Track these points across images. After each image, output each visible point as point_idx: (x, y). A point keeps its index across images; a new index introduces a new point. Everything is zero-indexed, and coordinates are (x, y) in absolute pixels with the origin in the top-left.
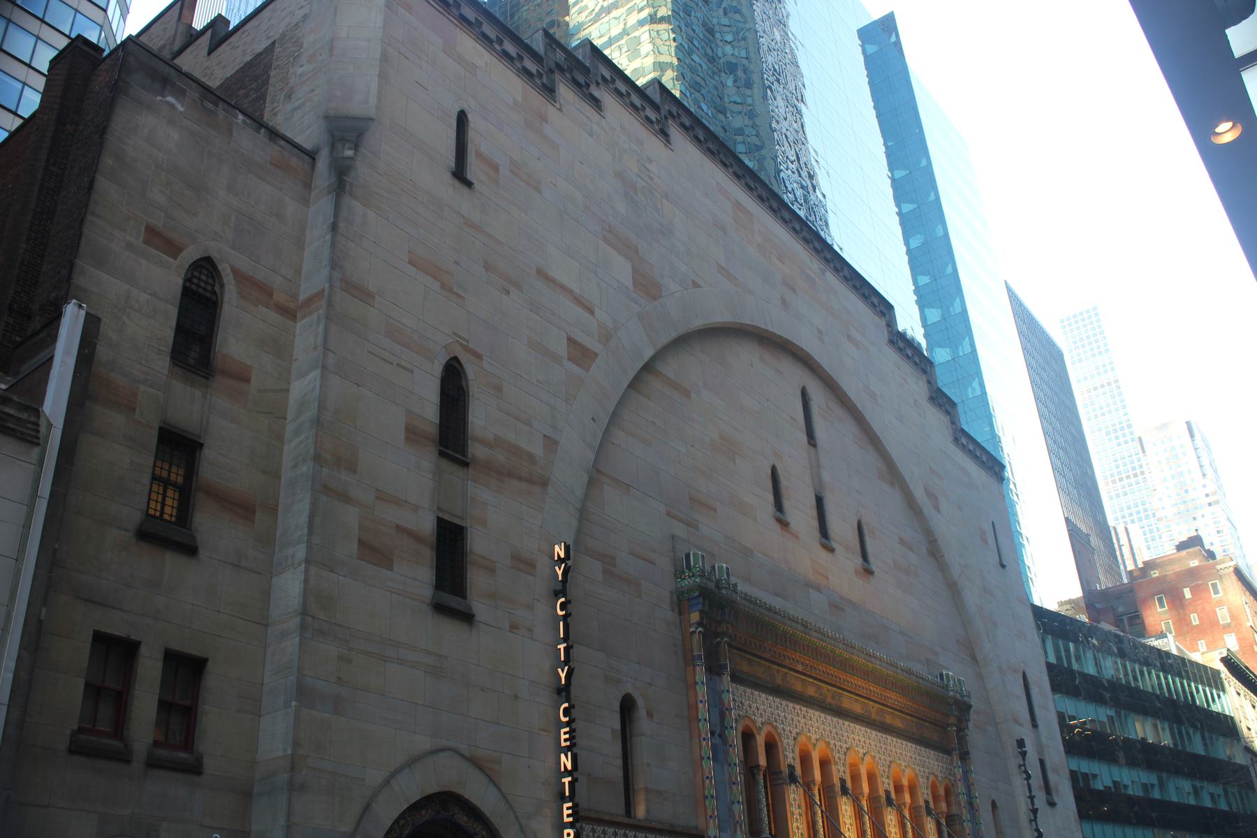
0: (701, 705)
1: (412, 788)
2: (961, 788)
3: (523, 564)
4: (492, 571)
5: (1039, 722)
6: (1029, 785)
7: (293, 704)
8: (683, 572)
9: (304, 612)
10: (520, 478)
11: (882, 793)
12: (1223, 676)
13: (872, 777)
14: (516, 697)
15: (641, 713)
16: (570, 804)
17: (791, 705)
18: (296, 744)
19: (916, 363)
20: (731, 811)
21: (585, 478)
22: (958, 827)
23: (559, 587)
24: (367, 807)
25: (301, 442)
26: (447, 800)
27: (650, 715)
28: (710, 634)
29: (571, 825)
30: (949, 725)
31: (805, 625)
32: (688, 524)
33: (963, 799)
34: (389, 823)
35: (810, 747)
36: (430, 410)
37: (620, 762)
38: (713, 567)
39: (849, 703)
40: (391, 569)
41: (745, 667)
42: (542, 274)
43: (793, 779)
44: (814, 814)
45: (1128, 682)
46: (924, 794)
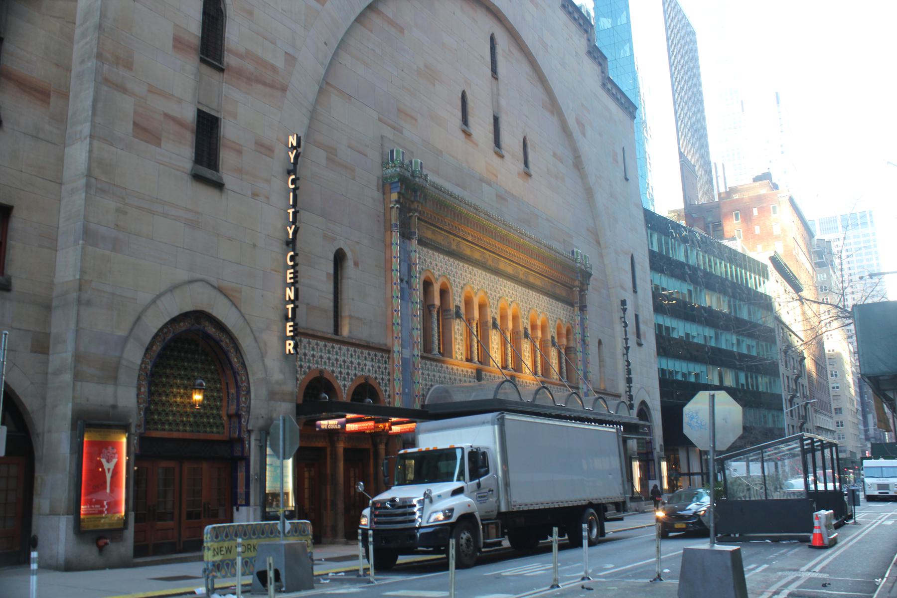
0: (394, 260)
1: (173, 307)
2: (578, 329)
3: (264, 148)
4: (239, 152)
5: (639, 289)
6: (626, 331)
7: (81, 242)
8: (388, 163)
9: (89, 175)
10: (264, 84)
12: (769, 269)
13: (515, 318)
14: (254, 246)
15: (349, 263)
16: (292, 324)
17: (461, 264)
18: (83, 272)
19: (580, 25)
20: (411, 335)
21: (317, 88)
22: (573, 356)
23: (291, 167)
24: (139, 319)
25: (87, 43)
26: (199, 316)
27: (356, 264)
28: (405, 209)
29: (292, 338)
31: (476, 209)
32: (394, 128)
33: (579, 337)
34: (155, 331)
35: (473, 295)
36: (193, 25)
37: (332, 296)
38: (411, 162)
39: (504, 266)
40: (159, 145)
41: (429, 235)
43: (458, 315)
44: (471, 340)
45: (705, 269)
46: (552, 331)
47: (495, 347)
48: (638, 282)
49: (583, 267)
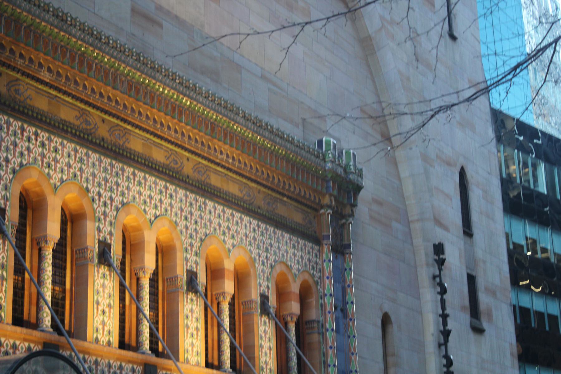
2: (329, 287)
6: (443, 302)
11: (181, 272)
13: (164, 252)
22: (315, 337)
30: (322, 207)
33: (329, 302)
35: (47, 191)
39: (137, 143)
47: (104, 302)
48: (475, 217)
49: (340, 171)
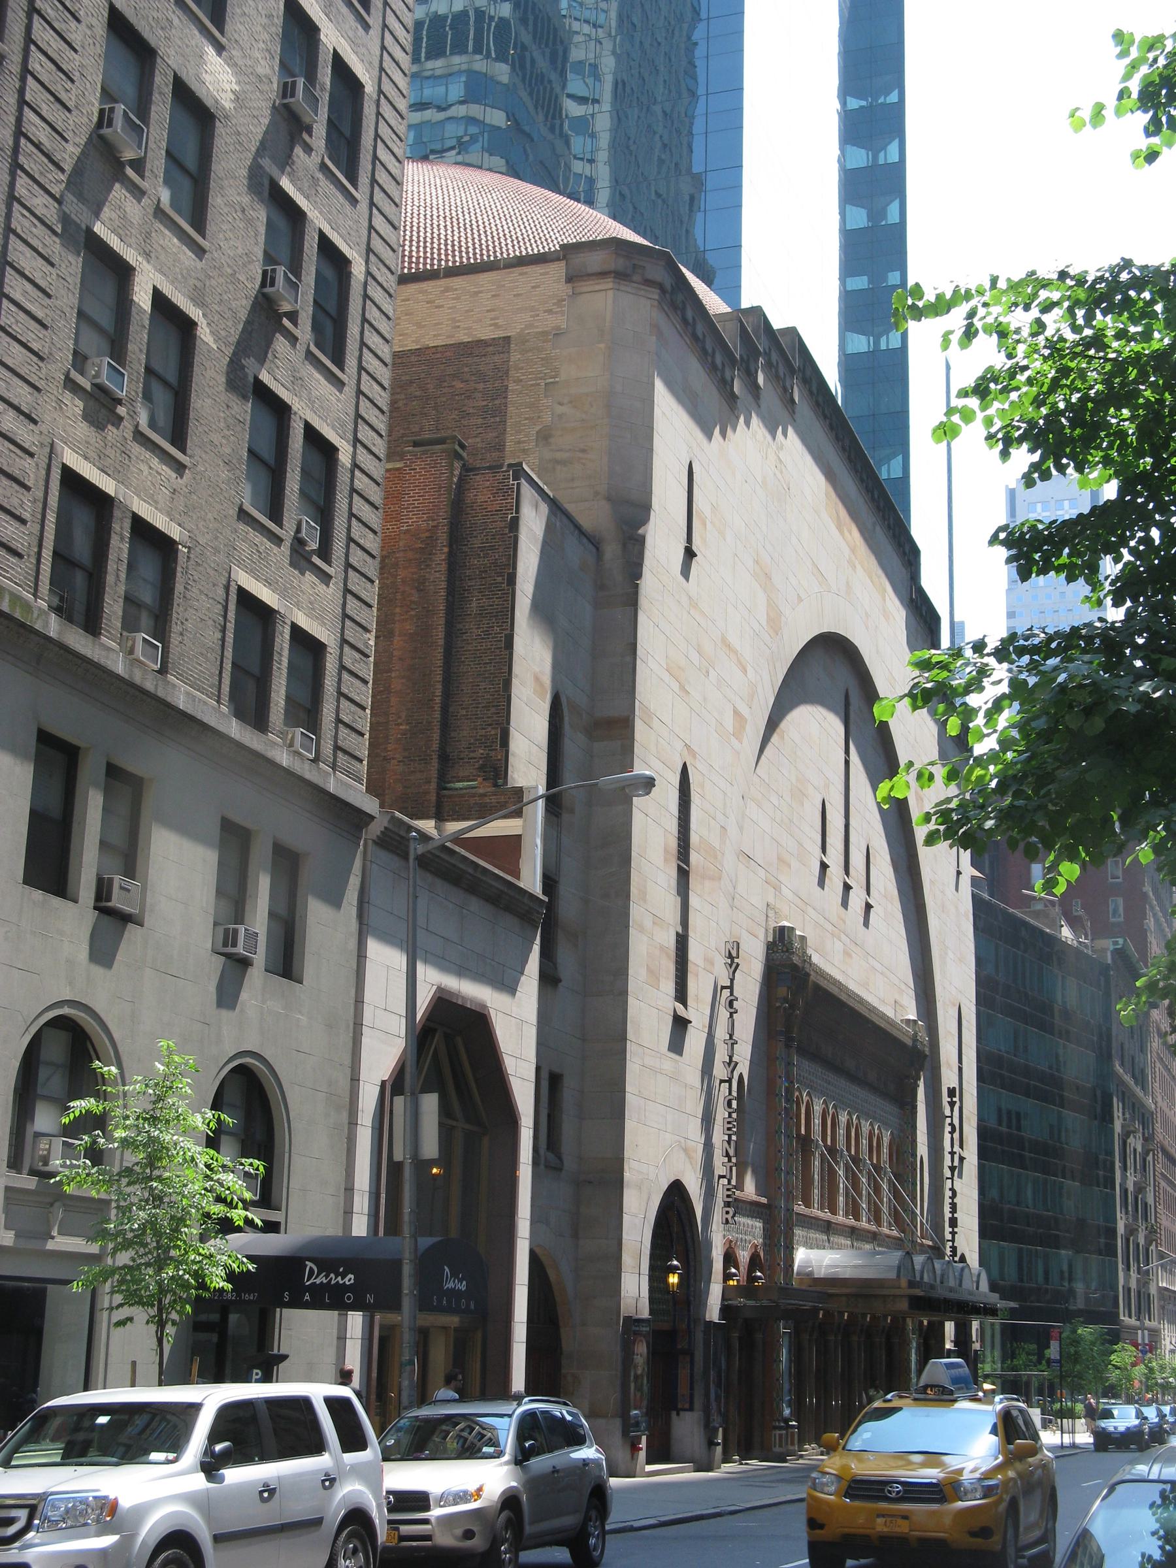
42: (724, 641)
